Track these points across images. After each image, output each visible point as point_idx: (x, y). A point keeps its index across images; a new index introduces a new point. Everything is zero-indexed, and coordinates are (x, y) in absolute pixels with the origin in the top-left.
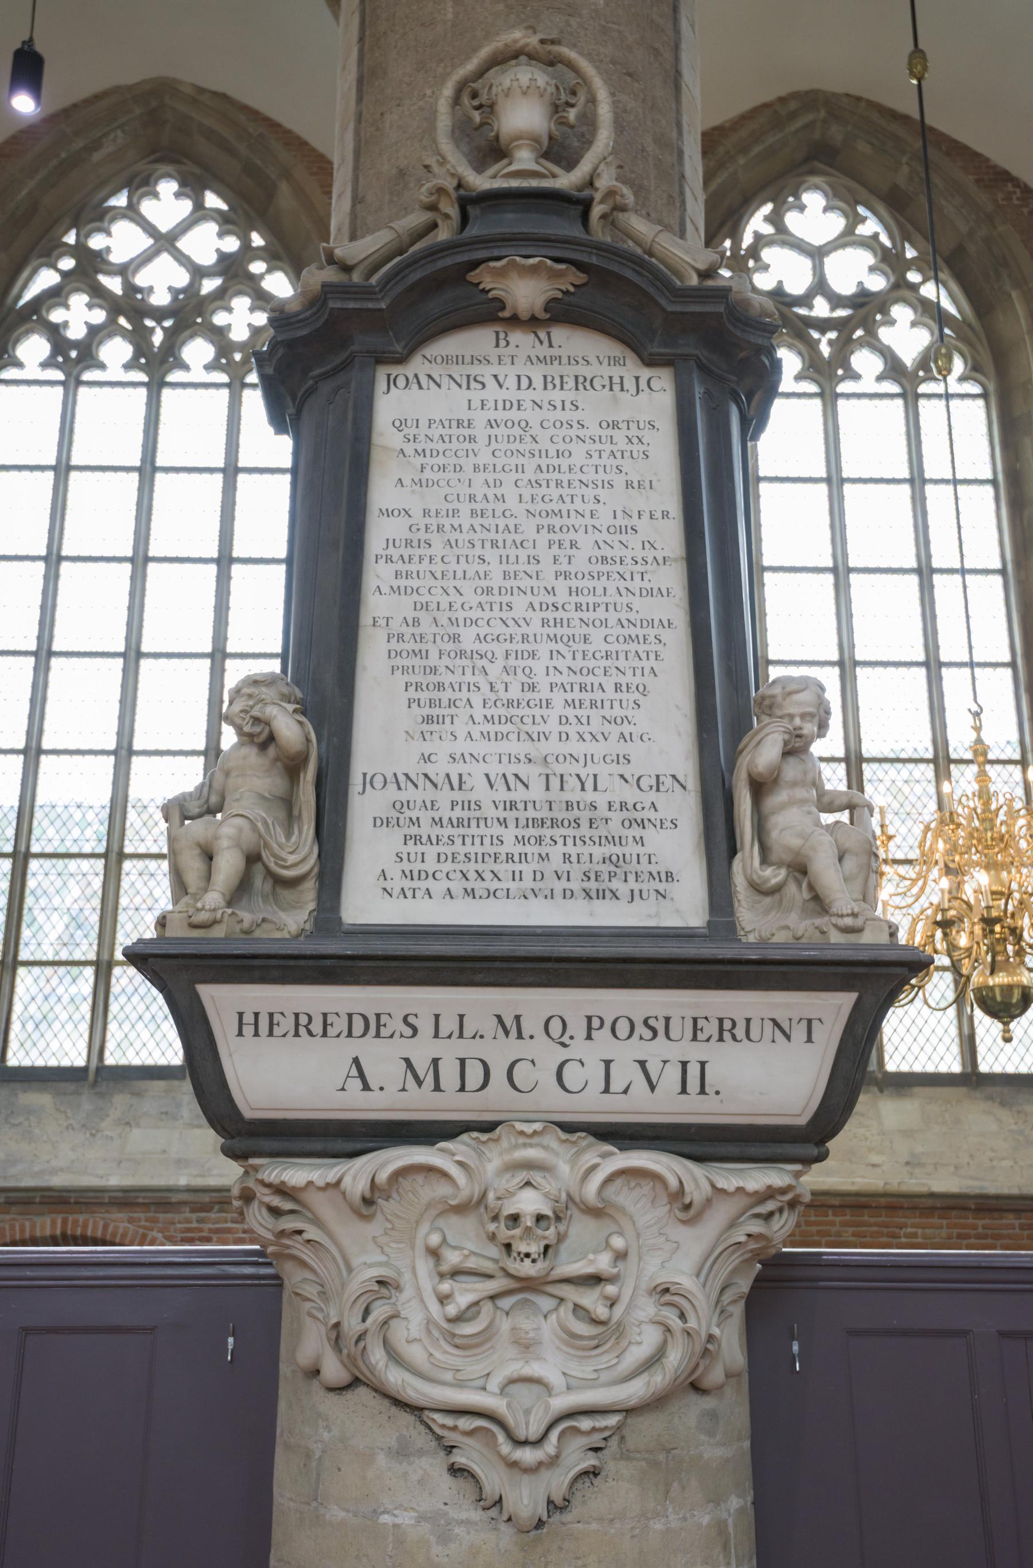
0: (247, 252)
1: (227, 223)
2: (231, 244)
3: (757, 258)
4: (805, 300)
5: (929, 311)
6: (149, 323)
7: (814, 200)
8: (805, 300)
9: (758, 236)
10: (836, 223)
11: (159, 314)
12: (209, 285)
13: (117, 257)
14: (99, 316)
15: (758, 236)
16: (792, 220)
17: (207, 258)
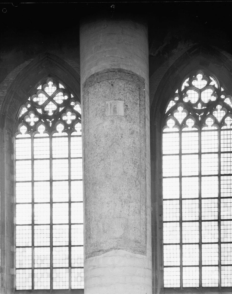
0: (70, 100)
1: (65, 92)
2: (66, 97)
3: (185, 93)
4: (196, 104)
5: (226, 107)
6: (48, 120)
7: (200, 76)
8: (196, 104)
9: (186, 87)
10: (205, 82)
11: (50, 118)
12: (61, 109)
13: (40, 103)
14: (37, 119)
15: (186, 87)
16: (194, 83)
17: (60, 102)
